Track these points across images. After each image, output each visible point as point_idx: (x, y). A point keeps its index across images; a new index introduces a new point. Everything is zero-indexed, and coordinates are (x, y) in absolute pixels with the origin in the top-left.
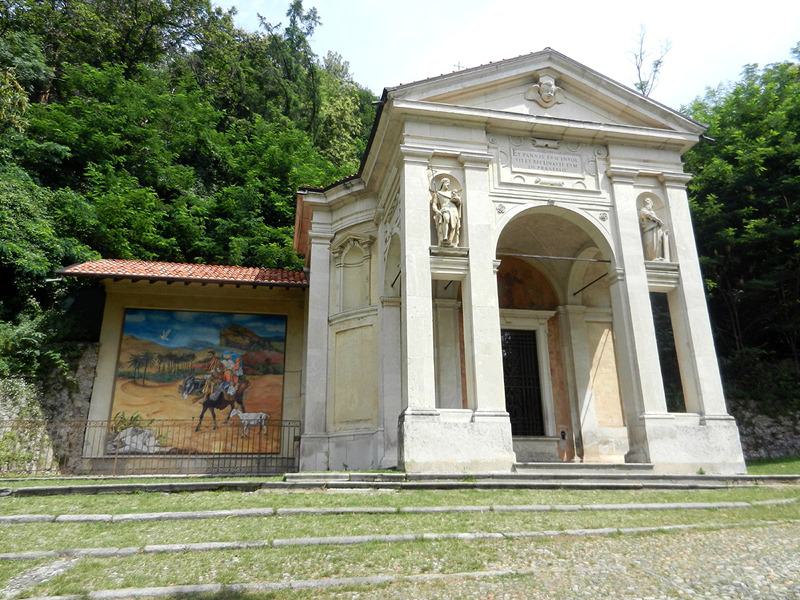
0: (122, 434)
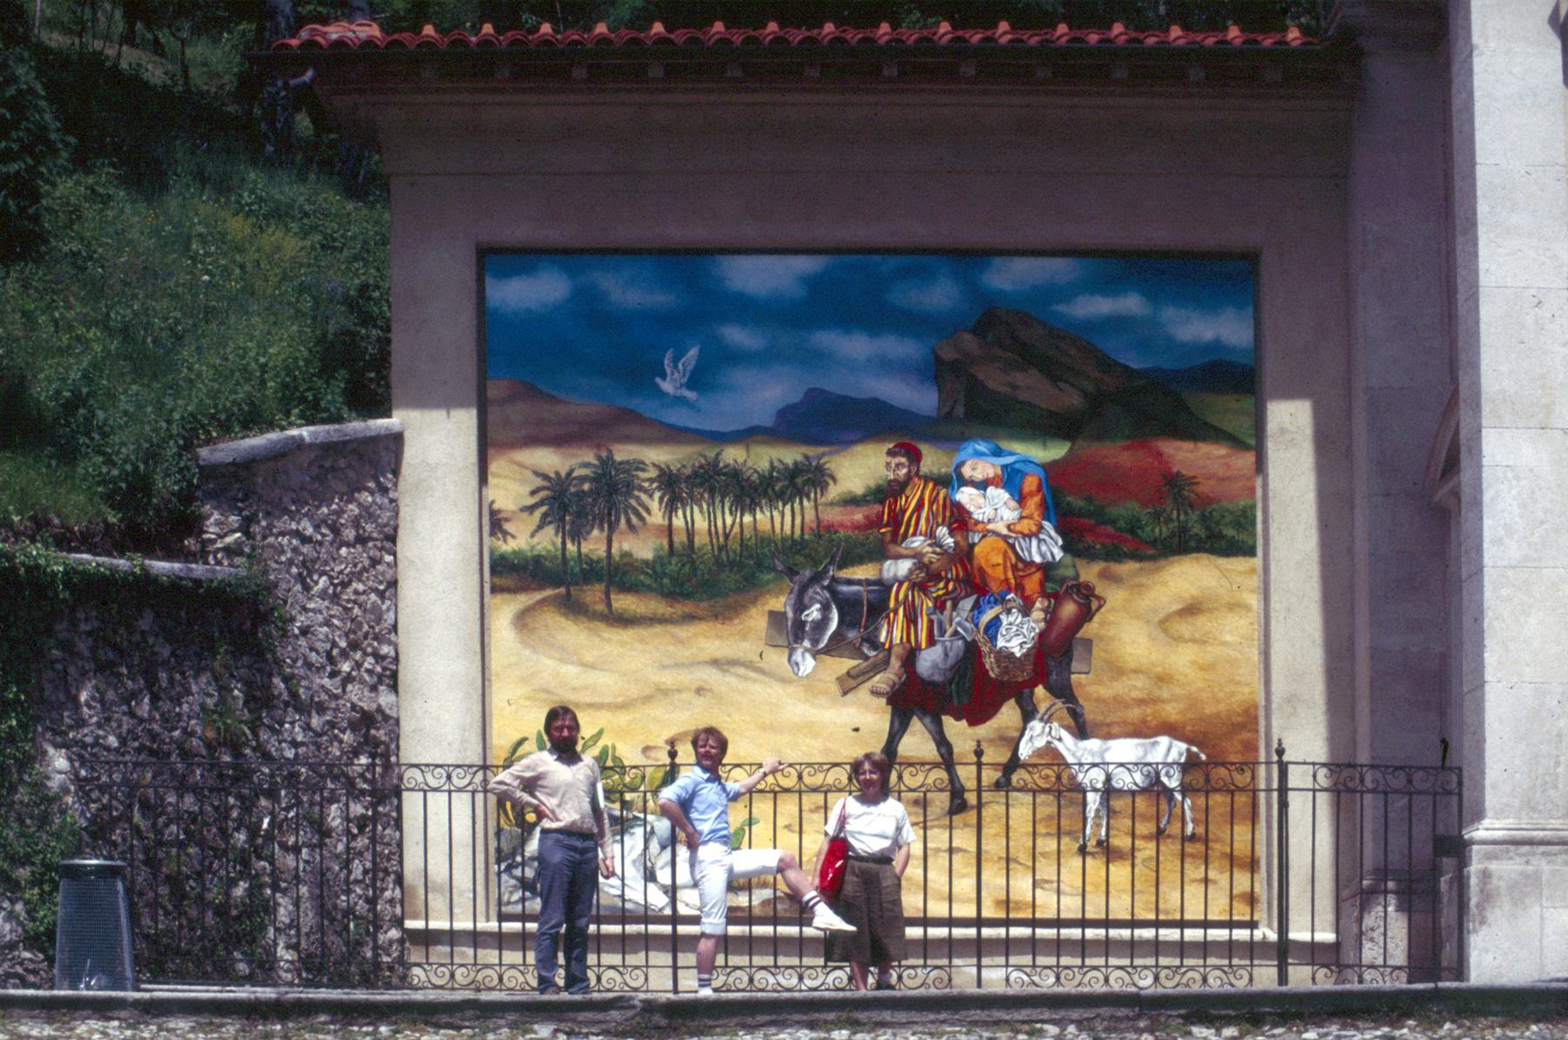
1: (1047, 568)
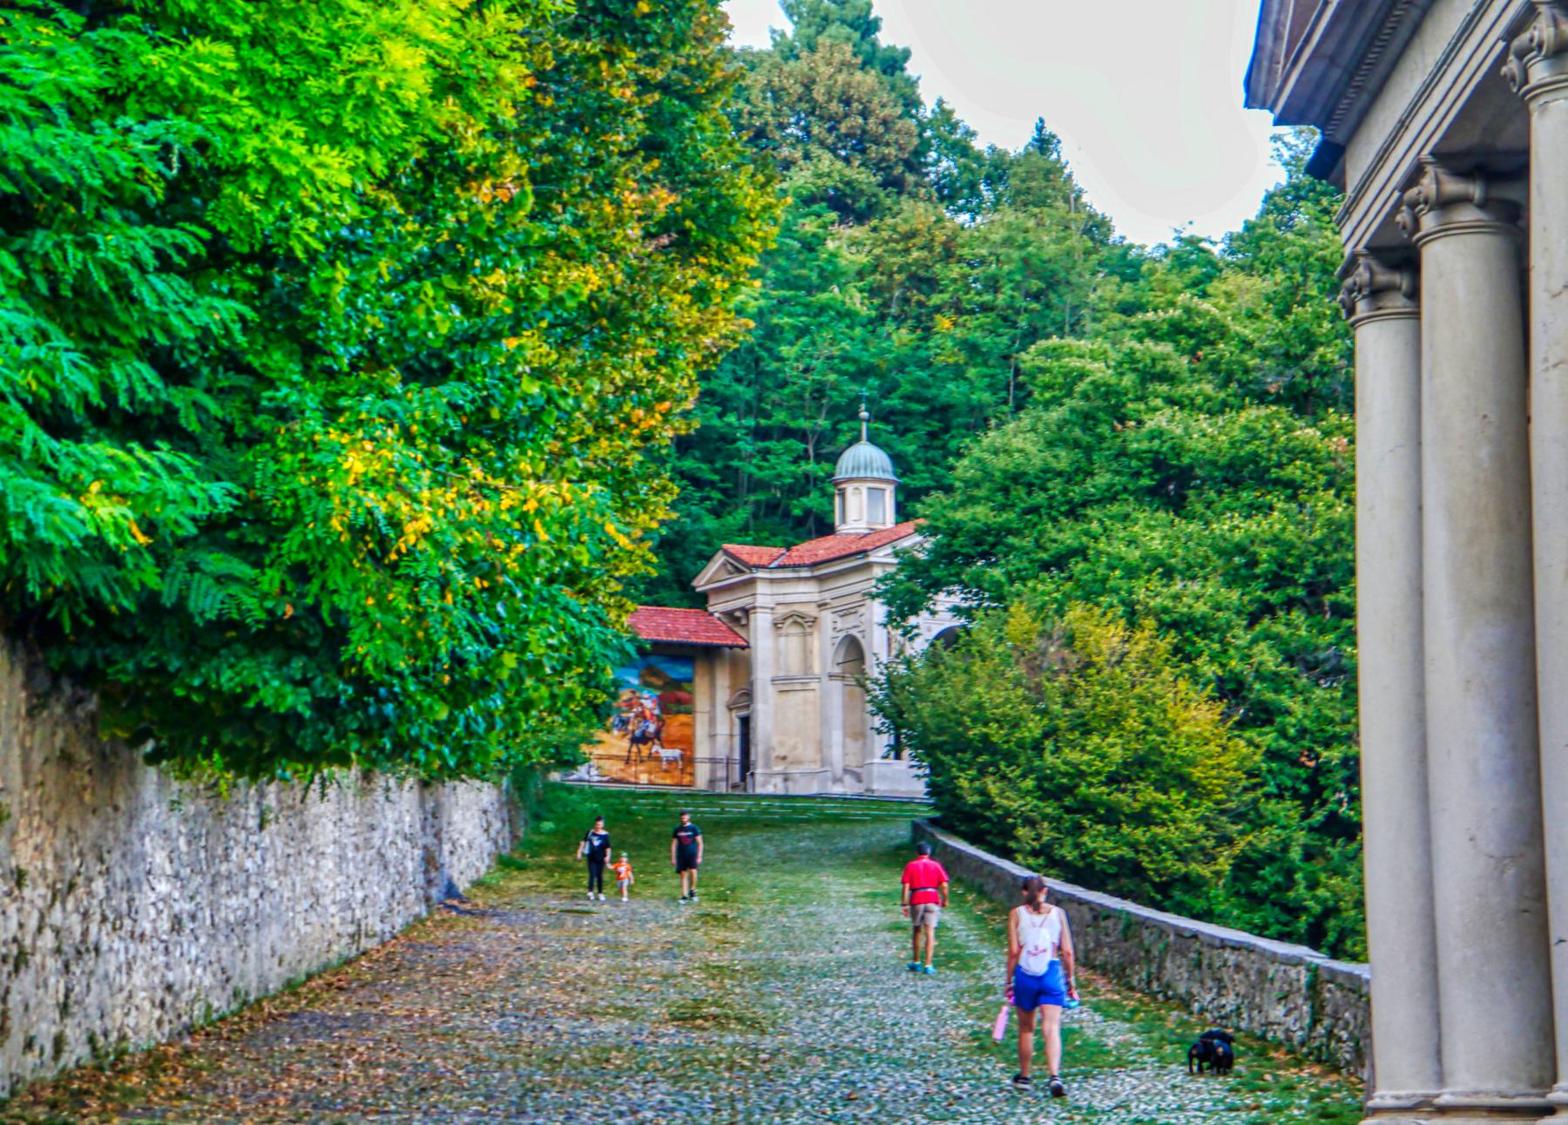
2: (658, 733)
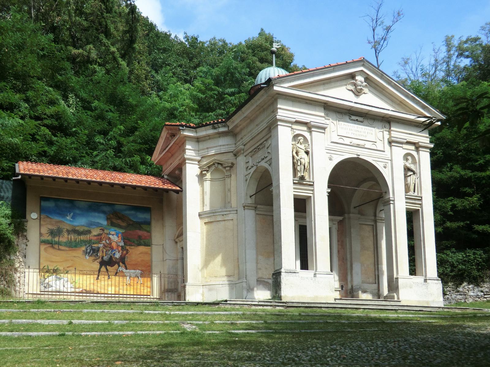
0: (47, 281)
1: (122, 246)
2: (122, 260)
